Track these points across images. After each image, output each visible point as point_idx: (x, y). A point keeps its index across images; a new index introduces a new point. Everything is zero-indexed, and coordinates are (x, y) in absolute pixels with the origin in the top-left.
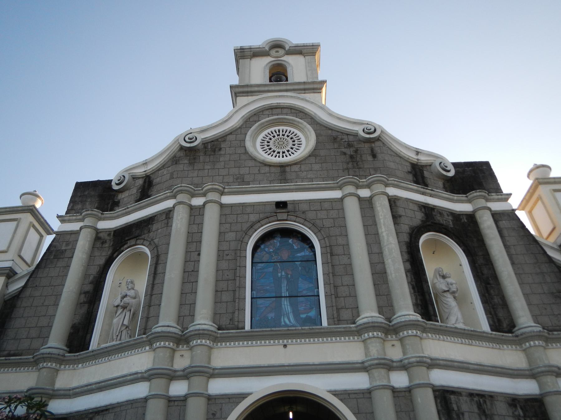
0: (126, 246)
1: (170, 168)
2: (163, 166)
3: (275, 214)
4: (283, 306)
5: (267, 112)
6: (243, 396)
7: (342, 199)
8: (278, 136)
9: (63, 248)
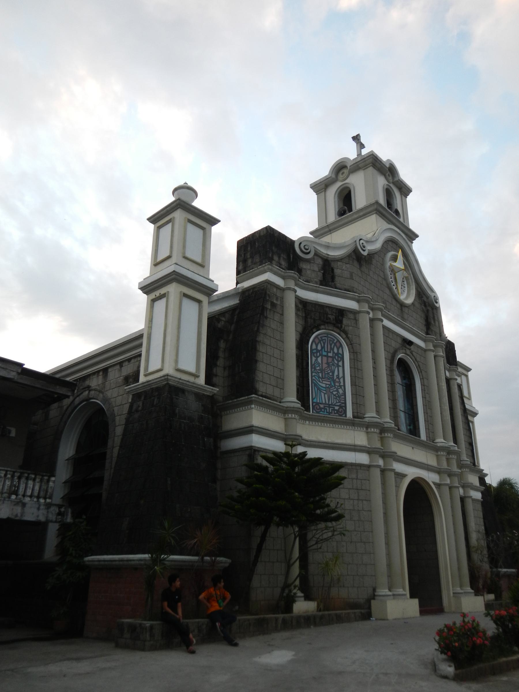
0: (322, 327)
1: (348, 266)
2: (342, 259)
3: (405, 348)
5: (390, 243)
7: (425, 351)
9: (275, 302)
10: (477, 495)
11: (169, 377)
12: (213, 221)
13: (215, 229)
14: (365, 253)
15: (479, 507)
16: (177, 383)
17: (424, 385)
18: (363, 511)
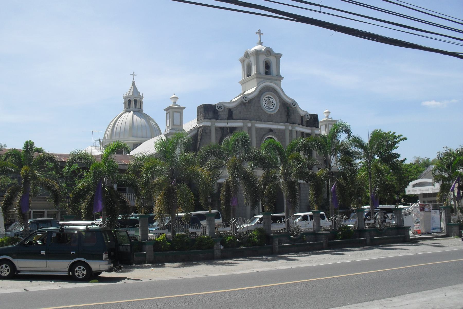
13: (184, 110)
14: (247, 101)
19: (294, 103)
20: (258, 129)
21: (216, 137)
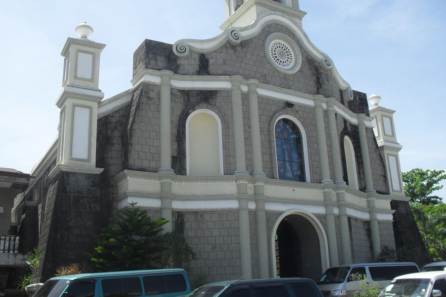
2: (215, 51)
4: (287, 166)
6: (281, 213)
8: (284, 50)
10: (390, 217)
11: (60, 167)
12: (101, 47)
14: (239, 41)
15: (391, 227)
16: (68, 170)
17: (310, 137)
18: (231, 244)
19: (328, 61)
20: (262, 100)
21: (172, 109)
